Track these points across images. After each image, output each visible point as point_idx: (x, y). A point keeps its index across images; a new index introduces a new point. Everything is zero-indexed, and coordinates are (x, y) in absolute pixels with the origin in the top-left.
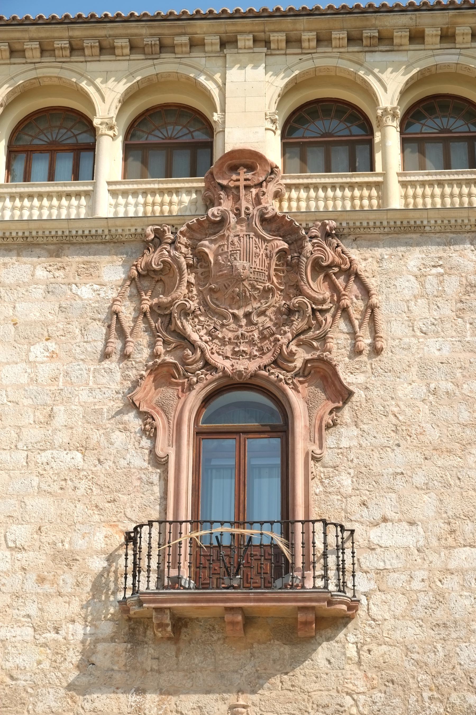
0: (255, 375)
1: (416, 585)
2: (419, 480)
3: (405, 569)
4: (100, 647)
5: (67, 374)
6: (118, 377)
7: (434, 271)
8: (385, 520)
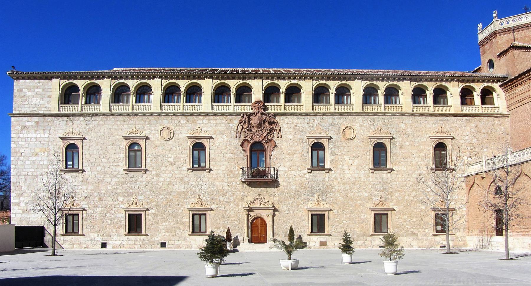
0: (261, 141)
1: (285, 176)
2: (286, 159)
3: (283, 174)
4: (238, 186)
5: (229, 140)
6: (238, 141)
7: (290, 123)
8: (281, 166)
